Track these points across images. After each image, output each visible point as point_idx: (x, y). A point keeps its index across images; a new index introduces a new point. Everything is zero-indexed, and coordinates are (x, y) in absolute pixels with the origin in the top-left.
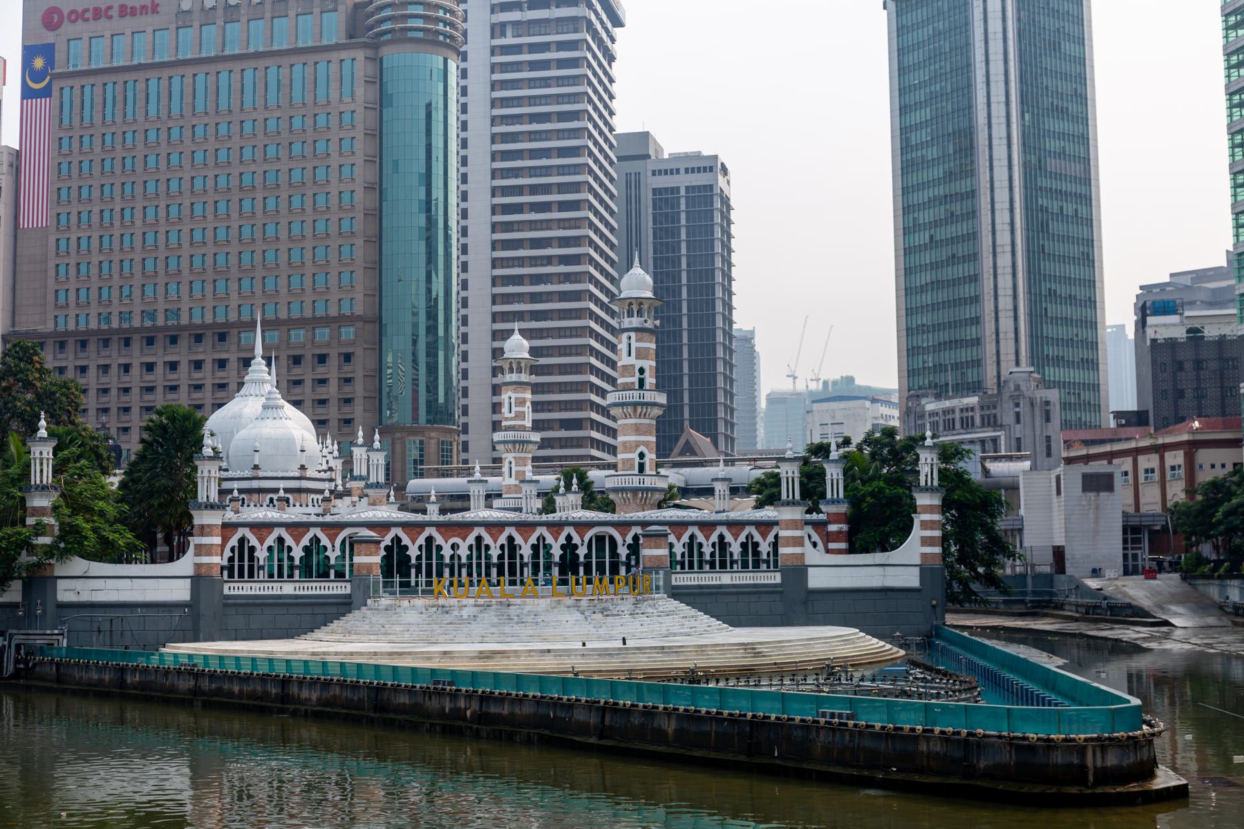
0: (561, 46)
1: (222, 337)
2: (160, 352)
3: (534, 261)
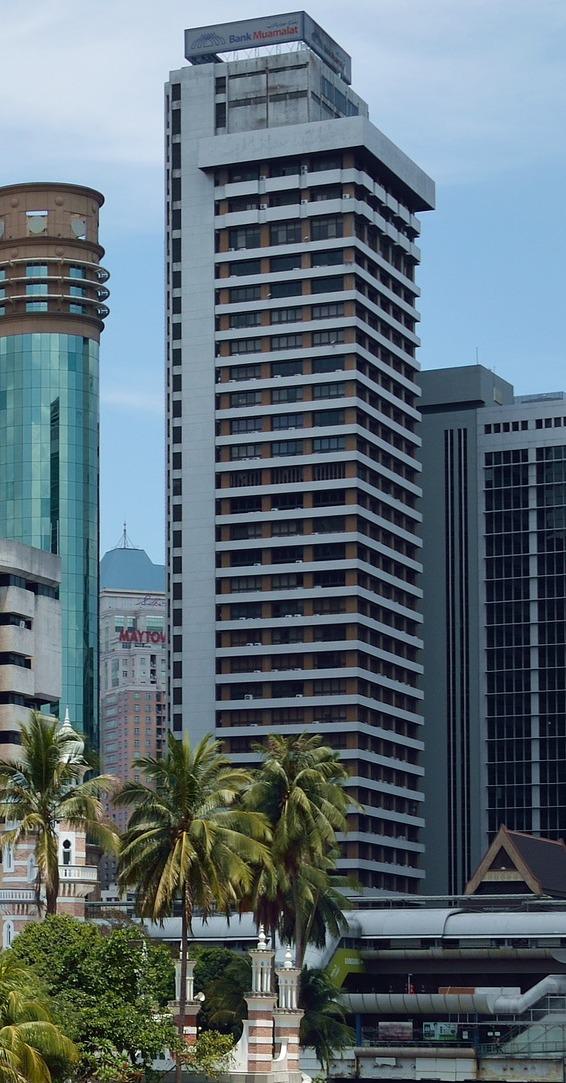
0: (317, 258)
3: (277, 582)
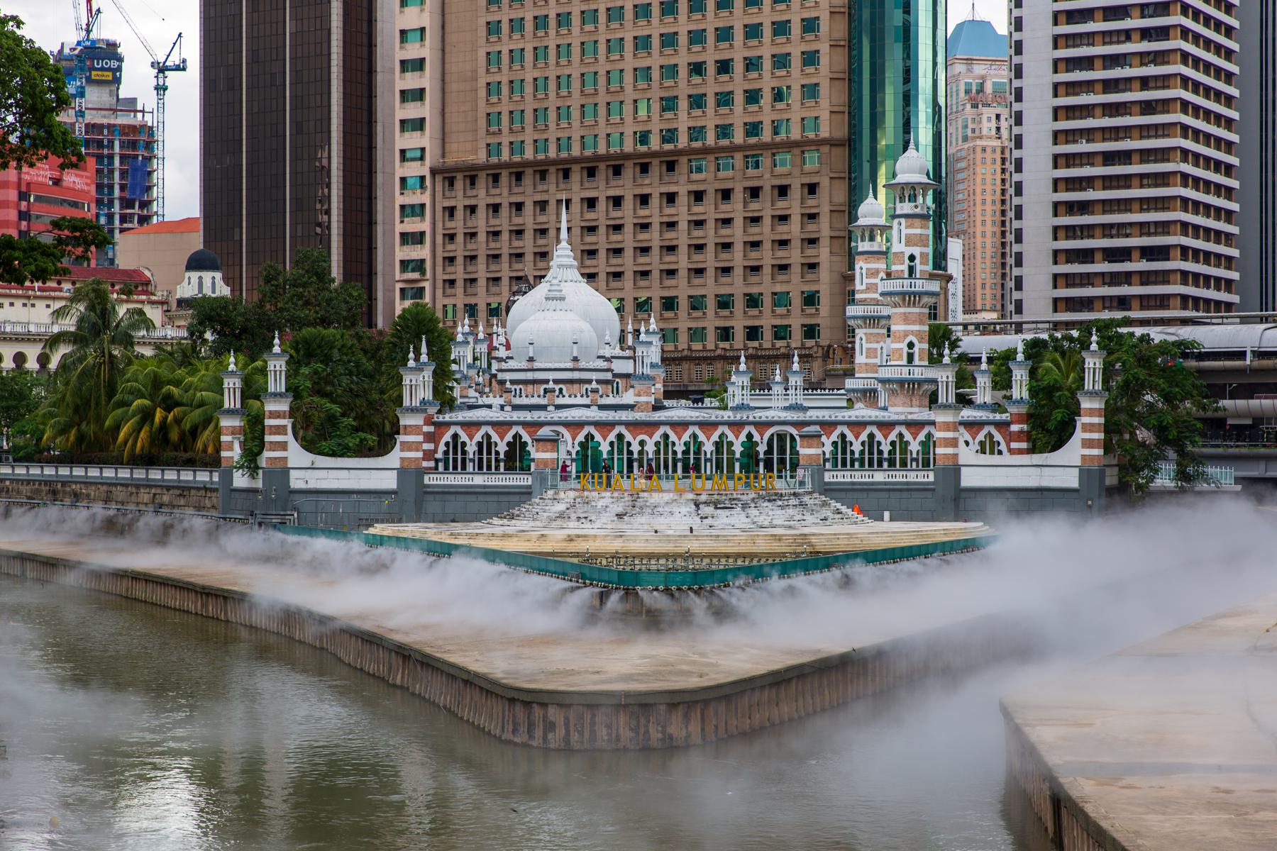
1: (671, 166)
2: (602, 184)
